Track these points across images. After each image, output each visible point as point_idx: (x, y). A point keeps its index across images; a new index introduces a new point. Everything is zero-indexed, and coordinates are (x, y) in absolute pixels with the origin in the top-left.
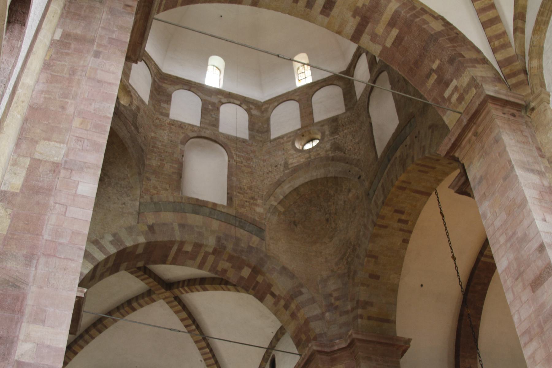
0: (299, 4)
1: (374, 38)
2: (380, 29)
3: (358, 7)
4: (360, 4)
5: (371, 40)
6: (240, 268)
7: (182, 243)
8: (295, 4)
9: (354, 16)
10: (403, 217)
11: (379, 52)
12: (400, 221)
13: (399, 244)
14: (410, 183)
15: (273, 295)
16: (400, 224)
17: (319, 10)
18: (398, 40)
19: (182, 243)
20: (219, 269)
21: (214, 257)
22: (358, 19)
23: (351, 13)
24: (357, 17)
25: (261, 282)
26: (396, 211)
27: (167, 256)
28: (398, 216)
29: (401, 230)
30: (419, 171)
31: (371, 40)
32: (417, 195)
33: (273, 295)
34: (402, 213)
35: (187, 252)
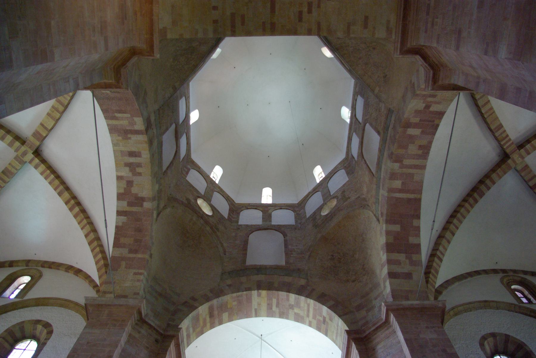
0: (141, 172)
1: (133, 123)
2: (125, 123)
3: (123, 138)
4: (120, 138)
5: (135, 124)
6: (411, 137)
7: (391, 190)
8: (142, 173)
9: (130, 138)
10: (305, 10)
11: (138, 118)
12: (310, 11)
13: (333, 3)
14: (264, 23)
15: (428, 107)
16: (313, 10)
17: (139, 159)
18: (120, 112)
19: (391, 190)
20: (420, 152)
21: (404, 160)
22: (129, 136)
23: (129, 140)
24: (129, 136)
25: (419, 119)
26: (300, 19)
27: (409, 200)
28: (305, 15)
29: (319, 6)
30: (243, 23)
31: (135, 124)
32: (277, 7)
33: (428, 107)
34: (301, 13)
35: (403, 183)
